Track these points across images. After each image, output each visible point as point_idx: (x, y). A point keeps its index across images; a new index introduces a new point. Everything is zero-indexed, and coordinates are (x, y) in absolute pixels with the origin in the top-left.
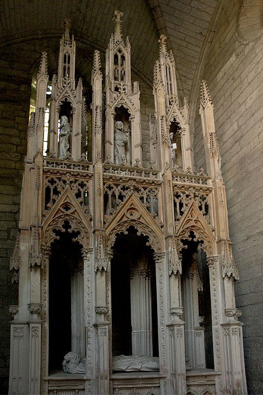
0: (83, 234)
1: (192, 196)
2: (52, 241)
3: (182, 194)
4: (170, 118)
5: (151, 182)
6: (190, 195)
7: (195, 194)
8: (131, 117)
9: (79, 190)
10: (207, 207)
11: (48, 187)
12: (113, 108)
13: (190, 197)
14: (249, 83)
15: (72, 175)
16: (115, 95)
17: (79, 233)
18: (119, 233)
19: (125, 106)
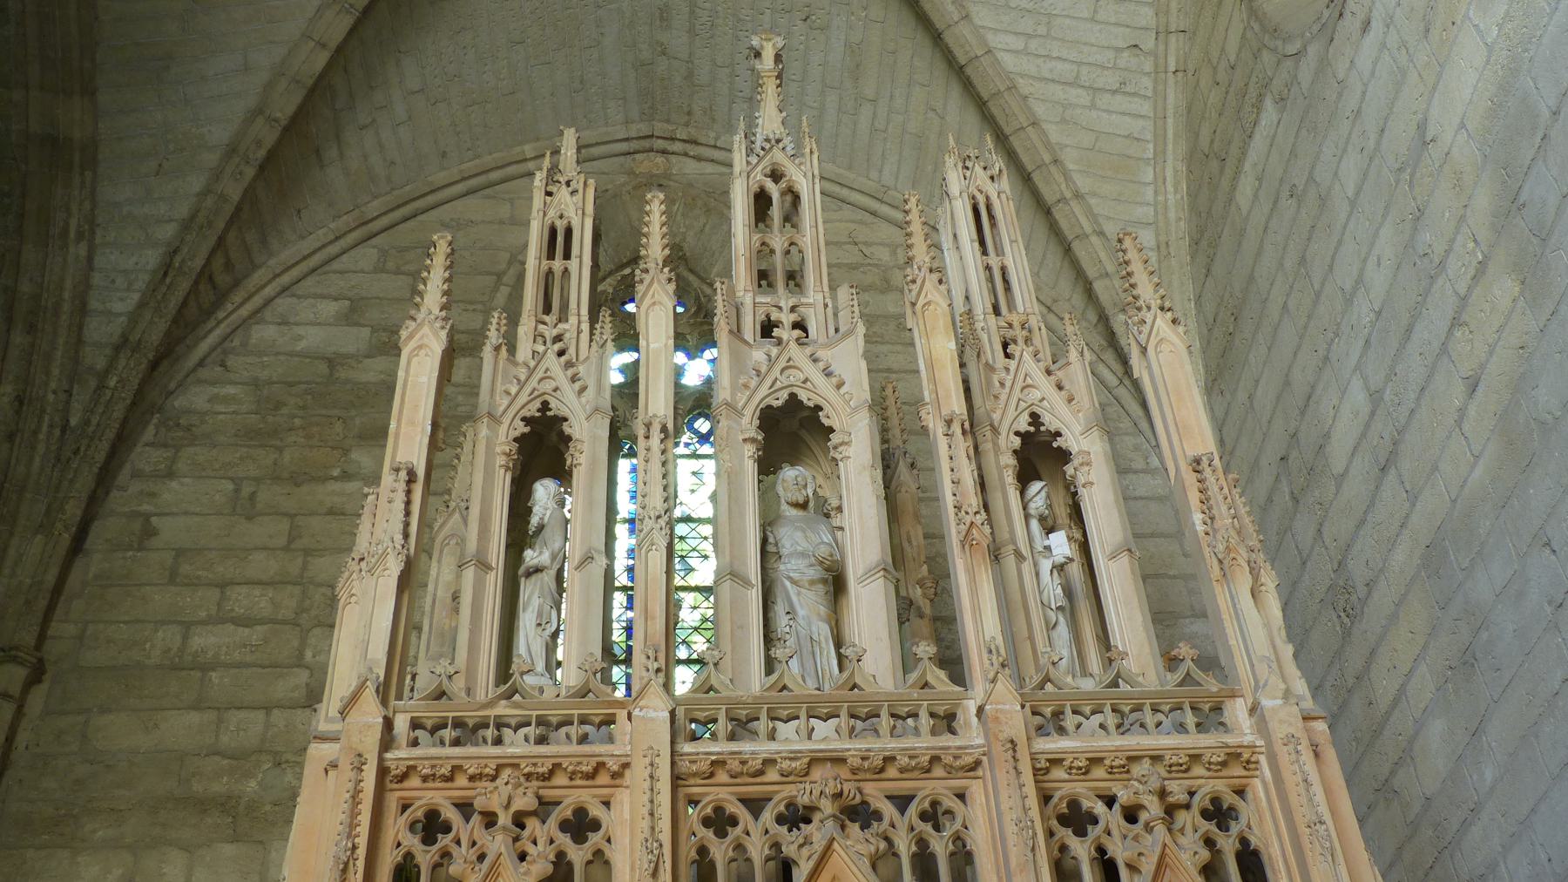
1: (1154, 808)
3: (1099, 808)
4: (1011, 413)
6: (1141, 807)
7: (1162, 794)
8: (835, 438)
9: (561, 855)
11: (409, 856)
12: (748, 412)
14: (1353, 203)
15: (528, 776)
16: (758, 355)
19: (803, 396)
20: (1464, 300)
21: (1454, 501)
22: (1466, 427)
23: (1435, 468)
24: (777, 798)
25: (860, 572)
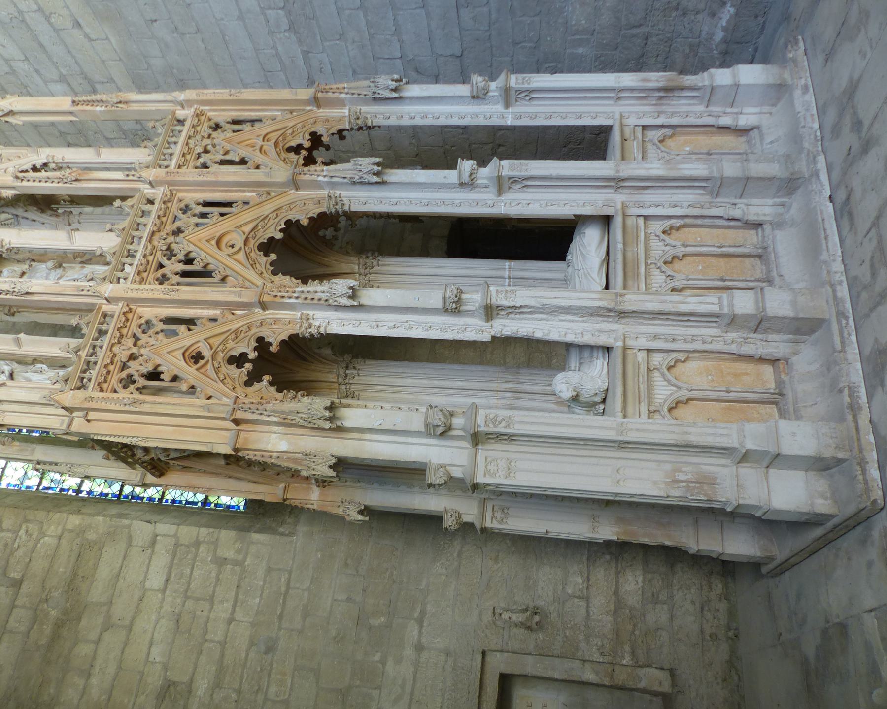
0: (265, 332)
2: (273, 389)
3: (201, 160)
5: (158, 221)
6: (205, 147)
10: (235, 122)
13: (209, 147)
15: (119, 342)
17: (260, 340)
18: (272, 268)
20: (40, 9)
21: (120, 60)
22: (93, 37)
23: (103, 61)
24: (160, 260)
25: (69, 243)
